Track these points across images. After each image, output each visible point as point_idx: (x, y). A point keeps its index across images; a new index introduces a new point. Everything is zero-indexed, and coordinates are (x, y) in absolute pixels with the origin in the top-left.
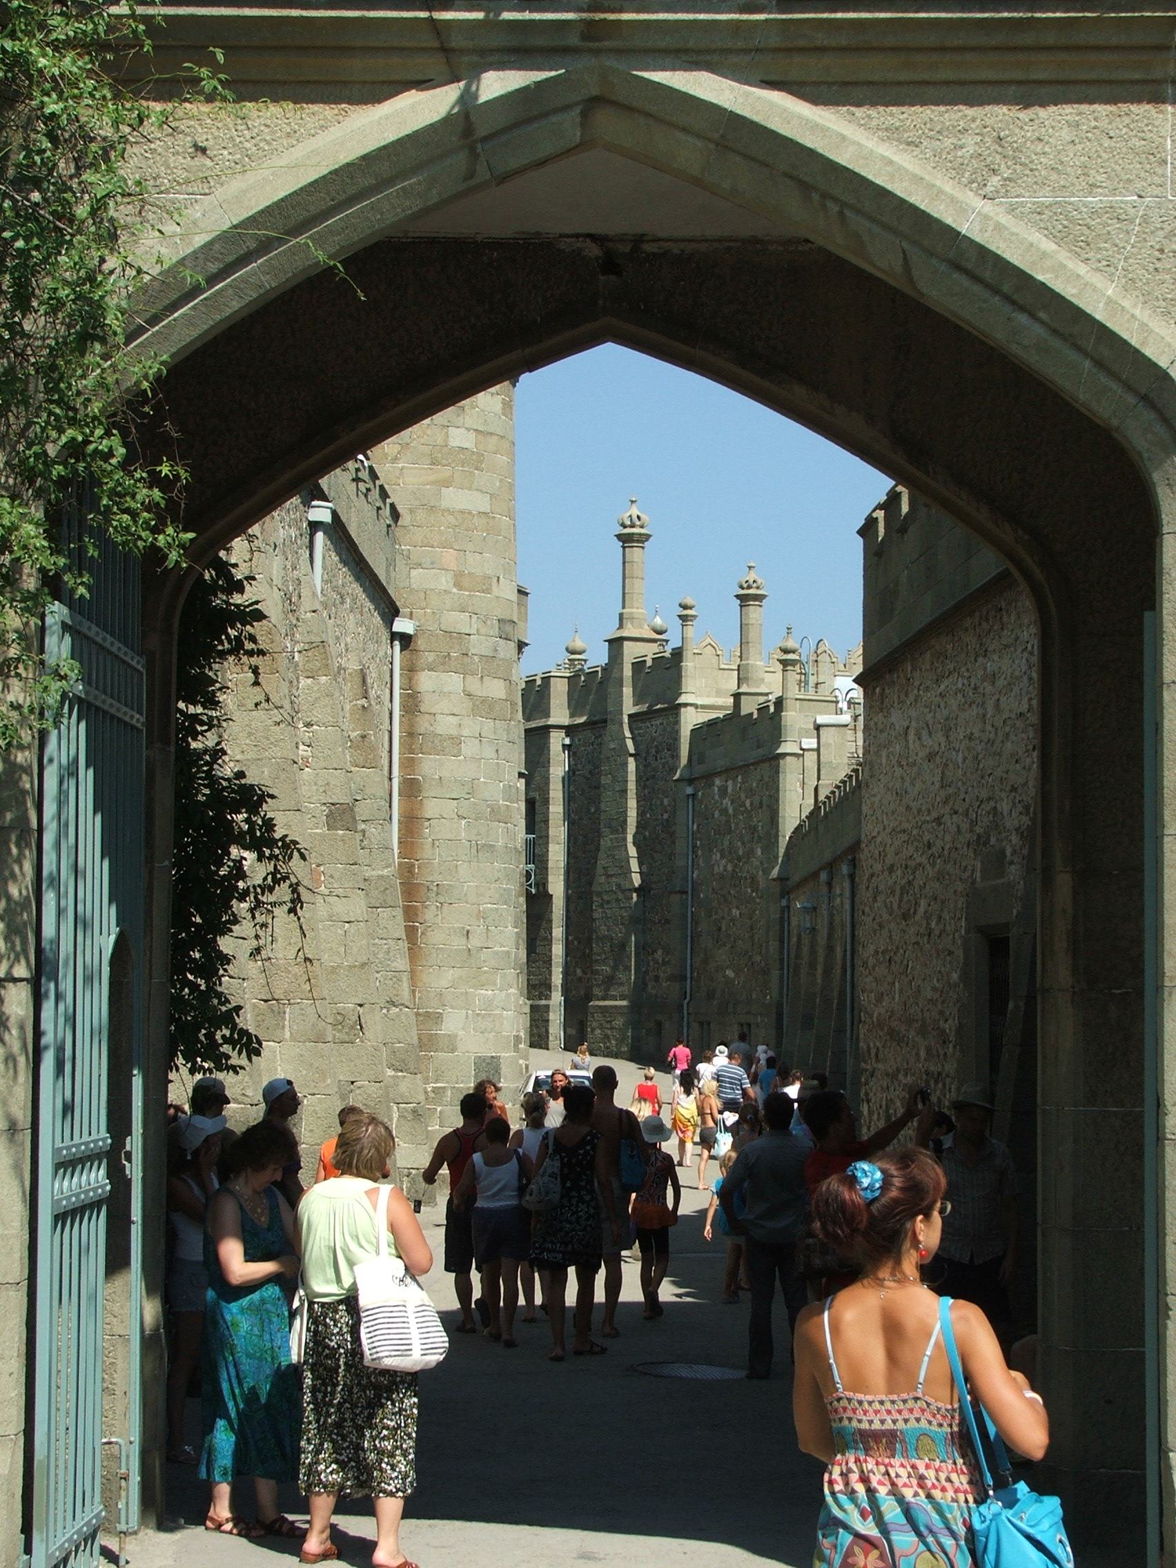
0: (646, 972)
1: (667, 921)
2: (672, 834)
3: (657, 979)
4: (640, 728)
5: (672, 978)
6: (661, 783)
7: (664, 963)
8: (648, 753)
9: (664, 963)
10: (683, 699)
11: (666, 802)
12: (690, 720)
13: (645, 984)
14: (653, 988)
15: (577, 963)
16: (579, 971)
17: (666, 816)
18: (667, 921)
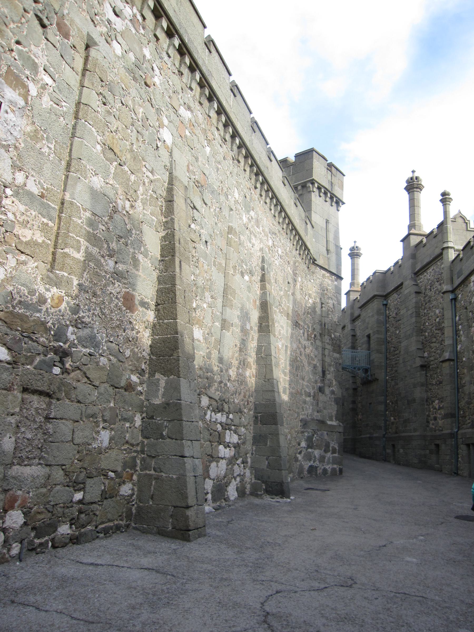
0: (428, 416)
1: (441, 382)
2: (442, 329)
3: (435, 419)
4: (421, 278)
5: (446, 416)
6: (434, 303)
7: (440, 408)
8: (426, 290)
9: (440, 408)
10: (445, 245)
11: (437, 311)
12: (452, 255)
13: (428, 422)
14: (433, 424)
15: (391, 414)
16: (392, 418)
17: (437, 320)
18: (441, 382)
